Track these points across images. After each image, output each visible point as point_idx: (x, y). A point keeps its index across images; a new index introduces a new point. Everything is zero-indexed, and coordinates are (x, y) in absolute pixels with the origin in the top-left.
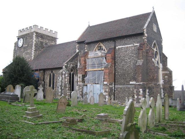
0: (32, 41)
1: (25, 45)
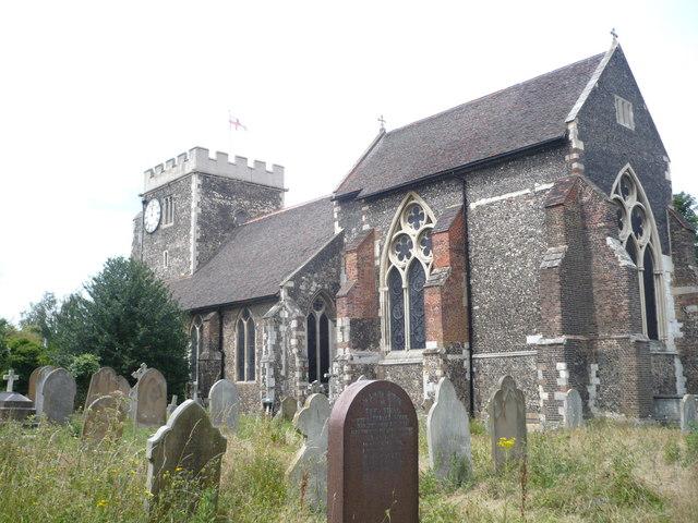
0: (189, 206)
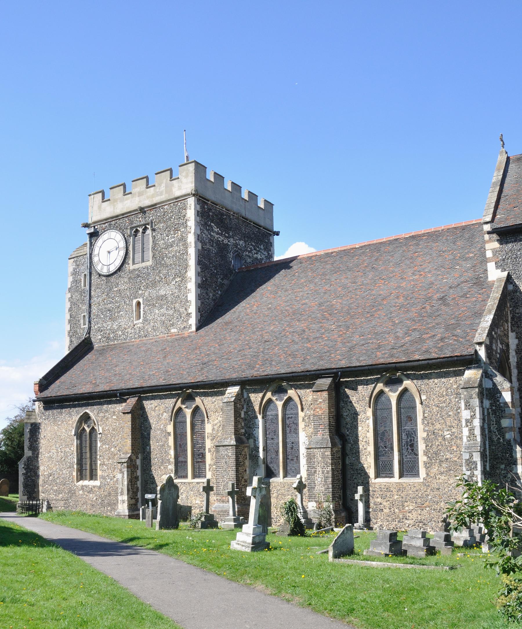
1: (134, 263)
